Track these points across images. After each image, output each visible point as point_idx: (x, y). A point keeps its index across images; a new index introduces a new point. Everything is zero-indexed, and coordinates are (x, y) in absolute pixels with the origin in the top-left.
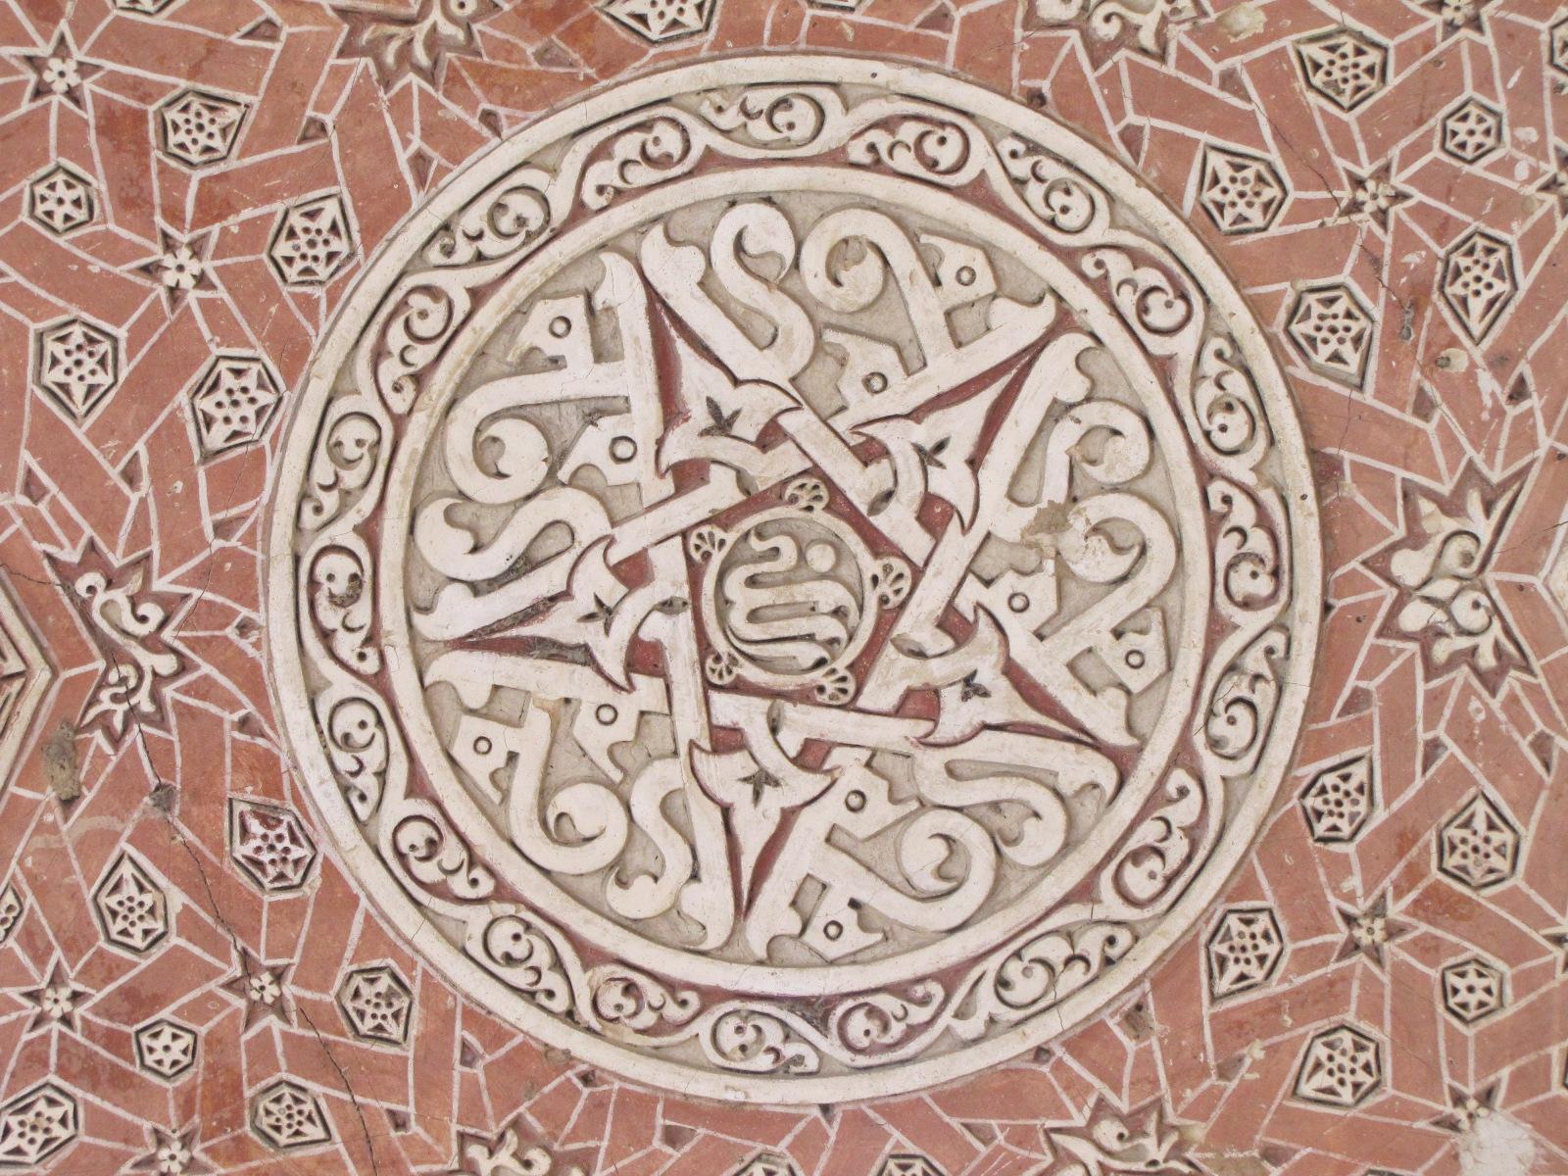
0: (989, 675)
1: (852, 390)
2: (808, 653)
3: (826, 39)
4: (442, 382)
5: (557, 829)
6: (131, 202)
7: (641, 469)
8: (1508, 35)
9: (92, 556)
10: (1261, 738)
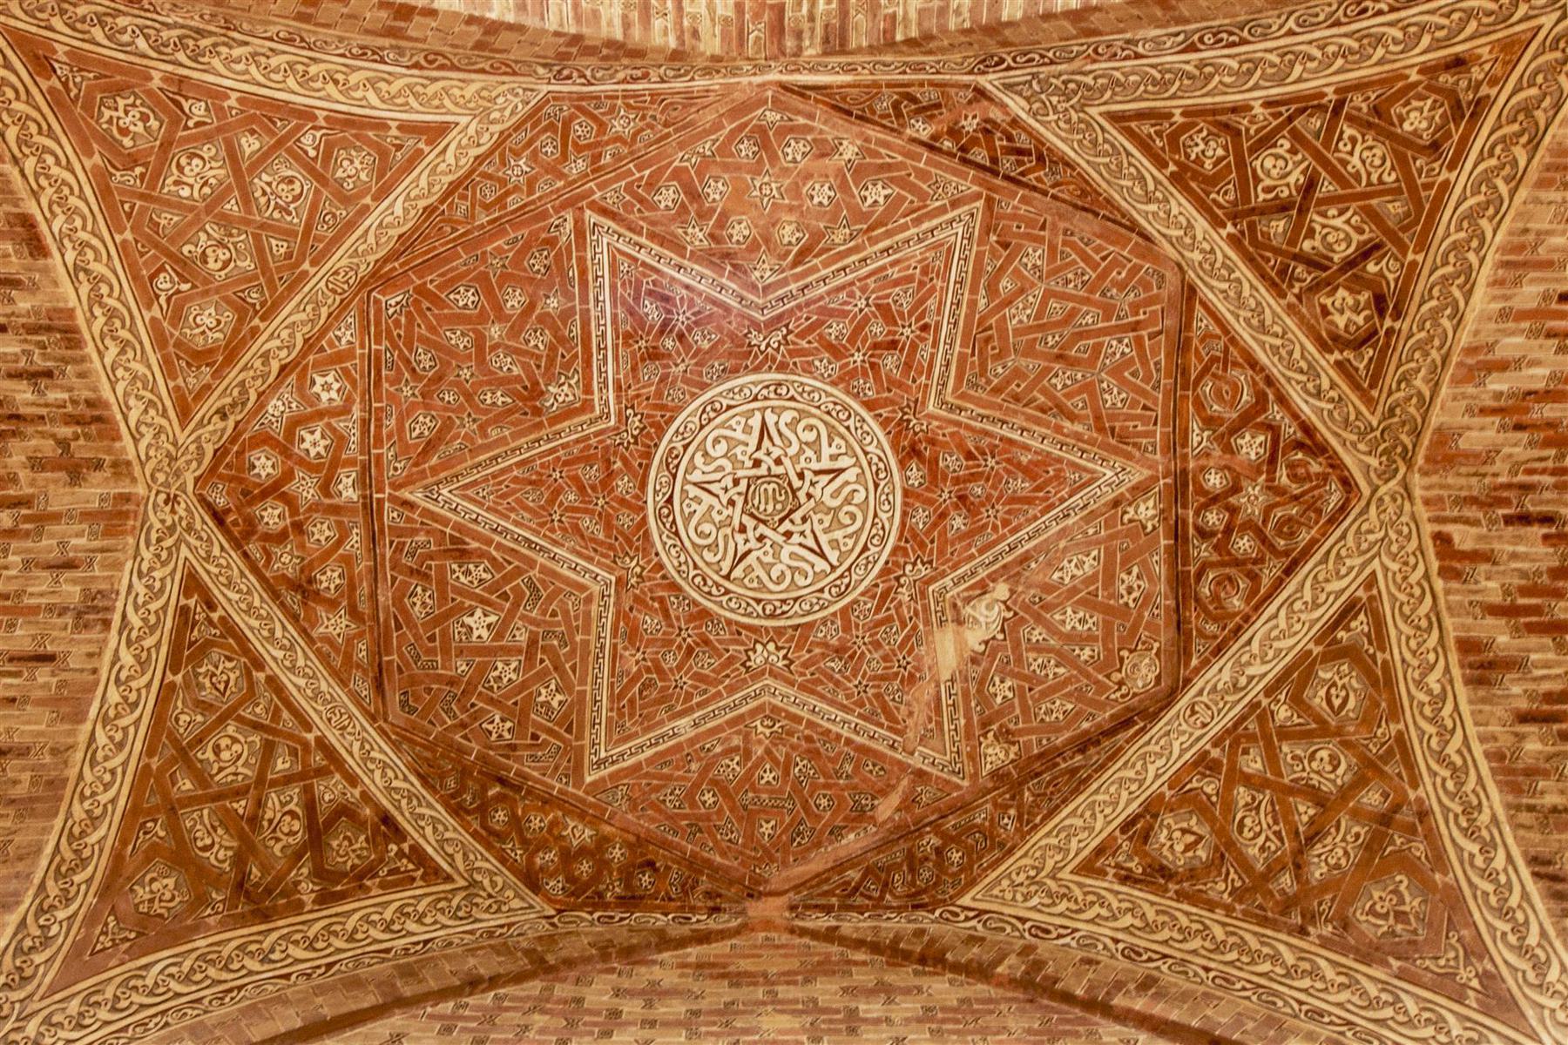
0: (748, 546)
1: (820, 516)
2: (756, 502)
3: (904, 514)
4: (827, 418)
5: (716, 441)
6: (875, 346)
7: (803, 464)
8: (897, 674)
9: (789, 332)
10: (732, 610)
